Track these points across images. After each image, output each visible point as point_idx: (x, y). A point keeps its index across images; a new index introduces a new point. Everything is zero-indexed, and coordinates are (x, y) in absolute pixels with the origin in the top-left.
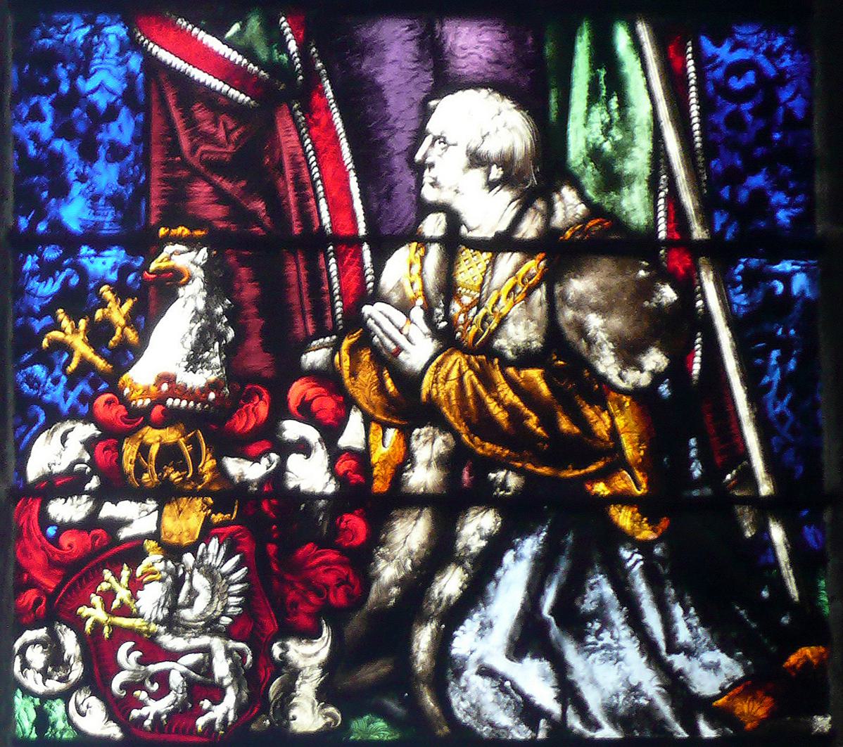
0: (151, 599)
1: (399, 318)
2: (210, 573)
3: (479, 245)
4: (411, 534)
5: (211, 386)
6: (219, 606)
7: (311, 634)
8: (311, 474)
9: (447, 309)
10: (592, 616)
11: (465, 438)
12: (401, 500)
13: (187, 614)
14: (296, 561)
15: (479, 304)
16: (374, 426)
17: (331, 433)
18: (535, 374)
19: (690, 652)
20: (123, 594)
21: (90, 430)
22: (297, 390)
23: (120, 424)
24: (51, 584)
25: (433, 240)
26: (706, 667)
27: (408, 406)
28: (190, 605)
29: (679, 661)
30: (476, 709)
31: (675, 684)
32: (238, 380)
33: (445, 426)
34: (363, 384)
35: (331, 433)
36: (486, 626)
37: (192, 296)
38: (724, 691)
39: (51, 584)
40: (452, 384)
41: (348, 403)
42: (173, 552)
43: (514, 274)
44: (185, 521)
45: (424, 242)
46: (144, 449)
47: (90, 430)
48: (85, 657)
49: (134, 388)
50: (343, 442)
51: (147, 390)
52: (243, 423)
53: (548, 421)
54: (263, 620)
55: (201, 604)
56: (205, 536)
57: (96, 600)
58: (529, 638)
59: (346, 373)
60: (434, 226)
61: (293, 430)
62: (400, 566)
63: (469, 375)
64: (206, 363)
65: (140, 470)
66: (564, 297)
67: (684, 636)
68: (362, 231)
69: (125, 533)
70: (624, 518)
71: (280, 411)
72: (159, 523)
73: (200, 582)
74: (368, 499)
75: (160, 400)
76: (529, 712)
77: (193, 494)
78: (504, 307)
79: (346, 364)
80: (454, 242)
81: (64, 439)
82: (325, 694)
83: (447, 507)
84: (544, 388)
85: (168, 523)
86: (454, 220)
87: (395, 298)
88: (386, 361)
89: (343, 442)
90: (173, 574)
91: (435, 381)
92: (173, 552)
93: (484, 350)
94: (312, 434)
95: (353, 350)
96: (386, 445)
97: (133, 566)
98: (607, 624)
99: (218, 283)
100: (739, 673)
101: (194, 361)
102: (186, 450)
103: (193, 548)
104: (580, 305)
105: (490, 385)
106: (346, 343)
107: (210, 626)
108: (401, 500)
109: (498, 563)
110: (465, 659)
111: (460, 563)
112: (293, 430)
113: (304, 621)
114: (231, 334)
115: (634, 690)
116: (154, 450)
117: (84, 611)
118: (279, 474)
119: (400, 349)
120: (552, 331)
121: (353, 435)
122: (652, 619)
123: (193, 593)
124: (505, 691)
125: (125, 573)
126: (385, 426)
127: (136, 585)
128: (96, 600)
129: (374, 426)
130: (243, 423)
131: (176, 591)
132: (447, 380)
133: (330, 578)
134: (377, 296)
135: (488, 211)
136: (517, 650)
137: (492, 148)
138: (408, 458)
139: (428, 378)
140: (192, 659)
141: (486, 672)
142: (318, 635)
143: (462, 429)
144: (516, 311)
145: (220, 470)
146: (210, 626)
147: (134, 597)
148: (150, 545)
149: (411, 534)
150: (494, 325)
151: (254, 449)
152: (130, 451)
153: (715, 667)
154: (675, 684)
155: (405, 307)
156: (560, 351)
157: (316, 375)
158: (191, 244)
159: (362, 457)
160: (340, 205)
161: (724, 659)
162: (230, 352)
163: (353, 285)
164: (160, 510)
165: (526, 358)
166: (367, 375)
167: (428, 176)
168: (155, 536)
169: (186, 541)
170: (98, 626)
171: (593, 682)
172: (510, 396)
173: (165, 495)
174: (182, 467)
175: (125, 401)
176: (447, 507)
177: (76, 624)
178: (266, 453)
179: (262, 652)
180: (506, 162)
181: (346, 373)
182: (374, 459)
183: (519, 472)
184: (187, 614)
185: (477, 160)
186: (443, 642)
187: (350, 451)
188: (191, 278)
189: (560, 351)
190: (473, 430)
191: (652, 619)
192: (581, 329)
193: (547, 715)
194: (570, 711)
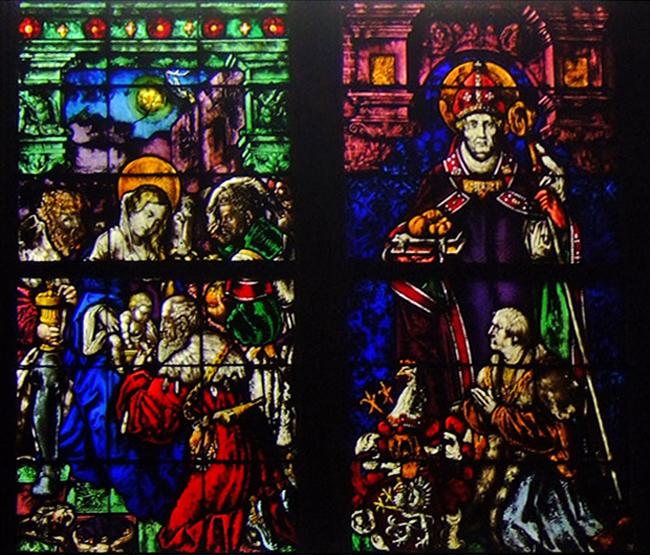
0: (399, 498)
1: (483, 394)
2: (419, 489)
3: (511, 366)
4: (489, 475)
5: (418, 419)
6: (422, 501)
7: (454, 514)
8: (453, 452)
9: (500, 390)
10: (551, 506)
11: (507, 439)
12: (487, 463)
13: (411, 504)
14: (449, 485)
15: (511, 388)
16: (475, 435)
17: (460, 437)
18: (530, 414)
19: (585, 519)
20: (389, 497)
21: (377, 436)
22: (449, 421)
23: (387, 433)
24: (364, 493)
25: (495, 365)
26: (591, 525)
27: (486, 427)
28: (412, 501)
29: (581, 523)
30: (511, 541)
31: (579, 531)
32: (427, 419)
33: (499, 434)
34: (471, 419)
35: (460, 437)
36: (515, 510)
37: (411, 385)
38: (596, 534)
39: (364, 493)
40: (502, 419)
41: (467, 426)
42: (406, 481)
43: (522, 377)
44: (411, 470)
45: (492, 366)
46: (396, 442)
47: (377, 436)
48: (376, 521)
49: (392, 419)
50: (465, 440)
51: (396, 421)
52: (430, 433)
53: (535, 432)
54: (437, 508)
55: (416, 501)
56: (417, 476)
57: (380, 499)
58: (527, 516)
59: (465, 414)
60: (494, 359)
61: (448, 435)
62: (485, 487)
63: (508, 415)
64: (417, 411)
65: (395, 449)
66: (540, 385)
67: (582, 513)
68: (471, 362)
69: (390, 474)
70: (562, 469)
71: (443, 429)
72: (401, 470)
73: (416, 492)
74: (474, 460)
75: (401, 424)
76: (528, 540)
77: (413, 461)
78: (520, 389)
79: (465, 411)
80: (503, 364)
81: (368, 439)
82: (459, 535)
83: (500, 465)
84: (533, 420)
85: (405, 471)
86: (502, 356)
87: (482, 386)
88: (480, 409)
89: (465, 440)
90: (406, 489)
91: (496, 417)
92: (406, 481)
93: (513, 406)
94: (454, 437)
95: (468, 407)
96: (479, 442)
97: (392, 487)
98: (556, 509)
99: (420, 380)
100: (601, 527)
101: (413, 410)
102: (410, 443)
103: (413, 480)
104: (546, 388)
105: (515, 420)
106: (466, 403)
107: (419, 509)
108: (487, 463)
109: (519, 486)
110: (507, 522)
111: (505, 486)
112: (448, 435)
113: (452, 507)
114: (425, 400)
115: (566, 534)
116: (399, 443)
117: (376, 503)
118: (443, 452)
119: (484, 405)
120: (535, 396)
121: (468, 437)
122: (572, 507)
123: (413, 497)
124: (521, 534)
125: (390, 490)
126: (479, 435)
127: (394, 494)
128: (380, 499)
129: (475, 435)
130: (430, 433)
131: (405, 495)
132: (501, 416)
133: (460, 492)
134: (476, 385)
135: (513, 353)
136: (525, 520)
137: (515, 329)
138: (488, 447)
139: (493, 416)
140: (412, 522)
141: (515, 526)
142: (457, 512)
143: (505, 435)
144: (523, 391)
145: (422, 450)
146: (419, 509)
147: (393, 499)
148: (399, 479)
149: (489, 475)
150: (516, 396)
151: (434, 443)
152: (391, 443)
153: (593, 525)
154: (579, 531)
155: (485, 389)
156: (539, 405)
157: (454, 414)
158: (412, 367)
159: (471, 445)
160: (463, 351)
161: (597, 523)
162: (425, 406)
163: (468, 382)
164: (401, 466)
165: (527, 408)
166: (473, 415)
167: (493, 340)
168: (400, 475)
169: (411, 477)
170: (381, 508)
171: (552, 531)
172: (522, 423)
173: (403, 461)
174: (408, 450)
175: (389, 424)
176: (500, 465)
177: (373, 508)
178: (438, 445)
179: (437, 518)
180: (519, 334)
181: (465, 414)
182: (476, 446)
183: (525, 452)
184: (411, 504)
185: (509, 334)
186: (500, 515)
187: (467, 443)
188: (412, 378)
189: (539, 405)
190: (509, 436)
191: (572, 507)
192: (546, 396)
193: (536, 542)
194: (544, 542)
